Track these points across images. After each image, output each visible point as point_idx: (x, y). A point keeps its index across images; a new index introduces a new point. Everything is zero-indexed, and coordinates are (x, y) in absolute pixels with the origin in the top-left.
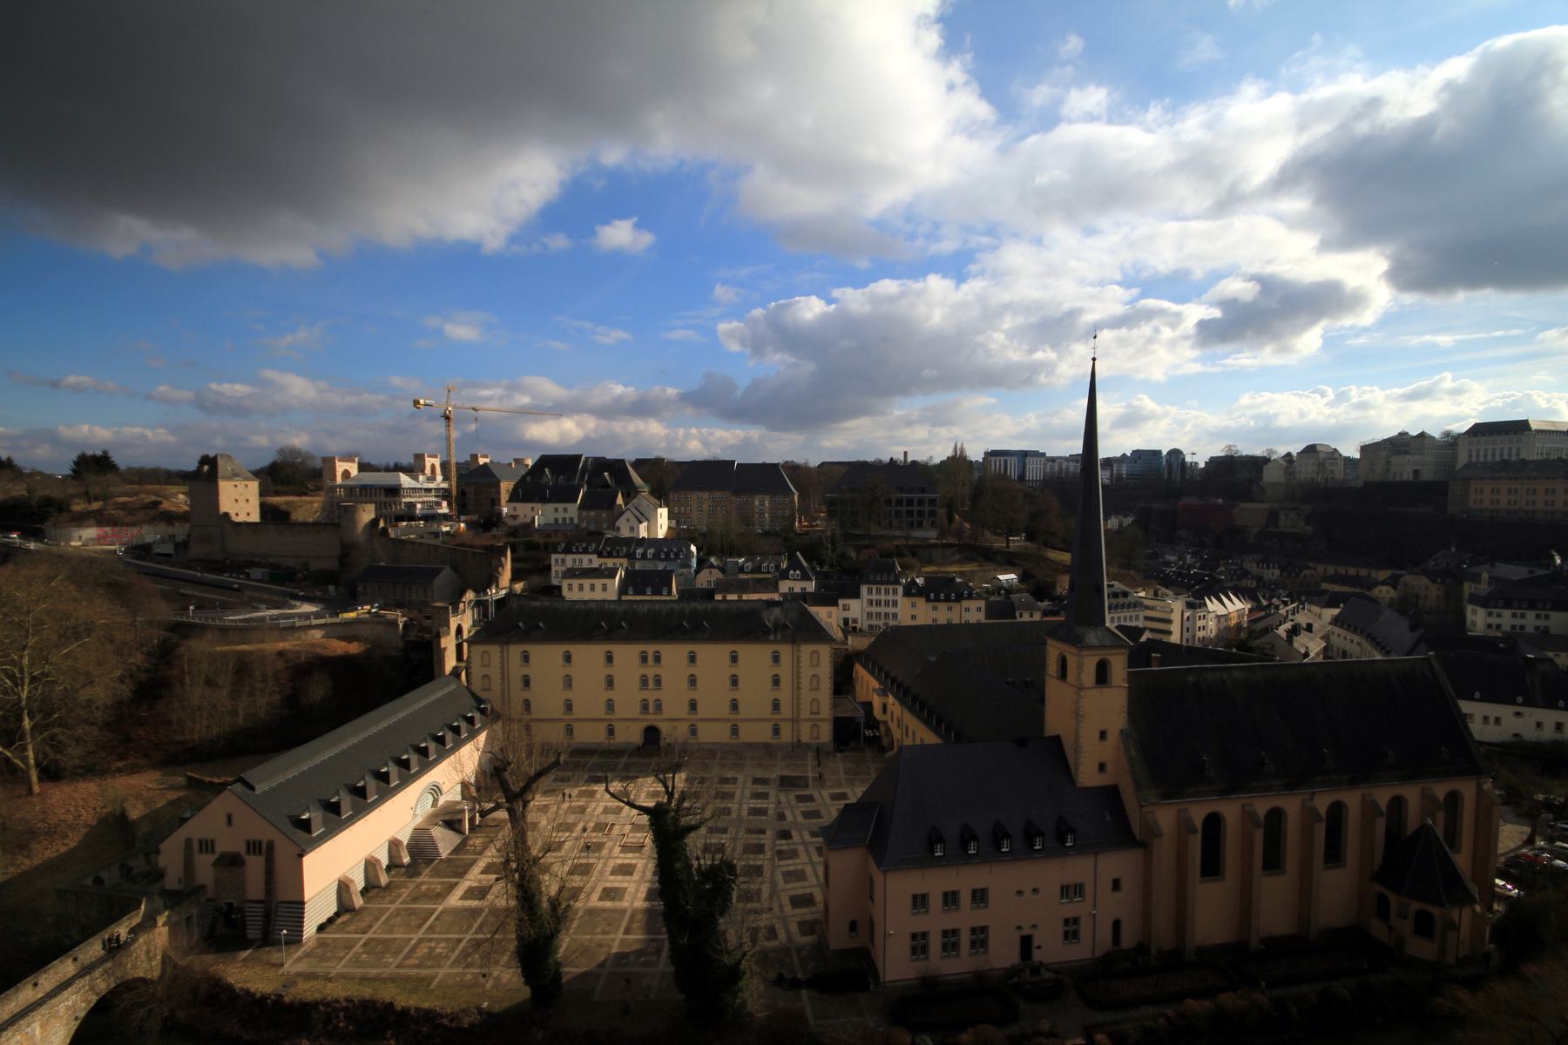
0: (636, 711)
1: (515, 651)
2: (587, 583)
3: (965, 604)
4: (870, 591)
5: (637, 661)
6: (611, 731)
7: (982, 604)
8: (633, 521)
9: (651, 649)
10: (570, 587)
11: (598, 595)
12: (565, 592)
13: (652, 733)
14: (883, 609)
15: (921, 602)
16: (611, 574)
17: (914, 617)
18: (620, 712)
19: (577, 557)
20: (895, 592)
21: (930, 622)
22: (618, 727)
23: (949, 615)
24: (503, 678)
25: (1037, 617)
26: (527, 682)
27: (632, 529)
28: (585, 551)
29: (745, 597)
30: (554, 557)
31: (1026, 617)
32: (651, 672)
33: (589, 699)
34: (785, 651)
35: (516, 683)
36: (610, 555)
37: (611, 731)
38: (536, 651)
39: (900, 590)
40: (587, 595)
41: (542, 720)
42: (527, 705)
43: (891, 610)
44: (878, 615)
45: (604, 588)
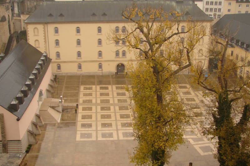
0: (113, 56)
1: (51, 28)
6: (100, 67)
9: (121, 25)
13: (121, 67)
14: (213, 7)
17: (229, 10)
18: (105, 57)
21: (237, 13)
22: (105, 65)
24: (45, 42)
26: (57, 42)
33: (89, 51)
37: (100, 67)
38: (61, 27)
41: (65, 62)
42: (58, 55)
43: (218, 7)
44: (211, 10)
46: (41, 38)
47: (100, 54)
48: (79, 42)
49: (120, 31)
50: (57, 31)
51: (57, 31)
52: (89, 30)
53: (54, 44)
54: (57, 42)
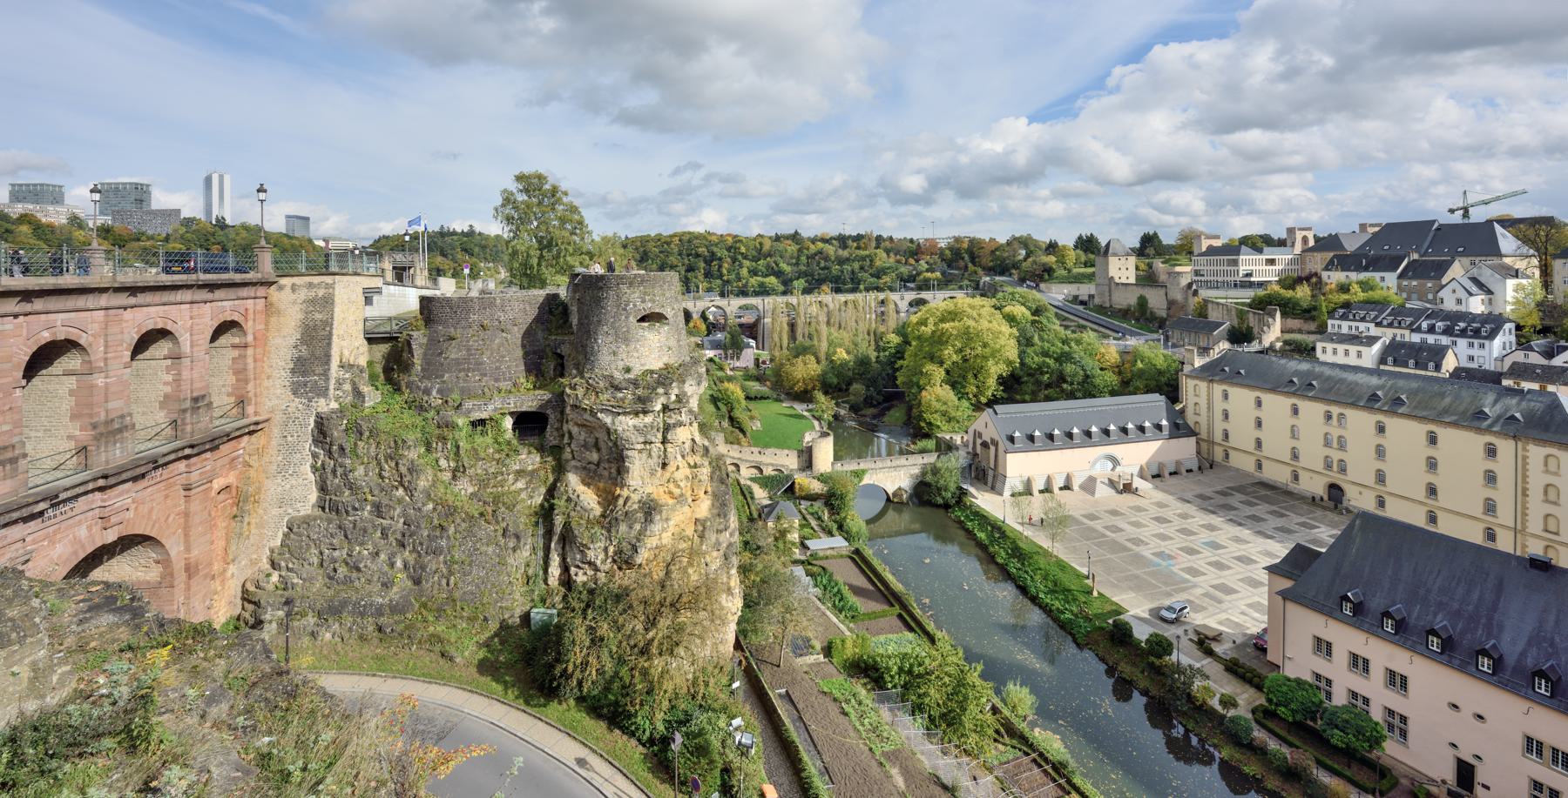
1: (1218, 389)
2: (1341, 348)
5: (1322, 419)
8: (1462, 294)
9: (1335, 410)
11: (1352, 360)
16: (1372, 340)
19: (1354, 324)
26: (1226, 416)
27: (1459, 301)
28: (1363, 319)
29: (1551, 388)
30: (1330, 322)
32: (1335, 432)
34: (1505, 447)
35: (1218, 416)
40: (1340, 359)
45: (1359, 355)
46: (1203, 402)
49: (1335, 417)
50: (1226, 396)
51: (1226, 396)
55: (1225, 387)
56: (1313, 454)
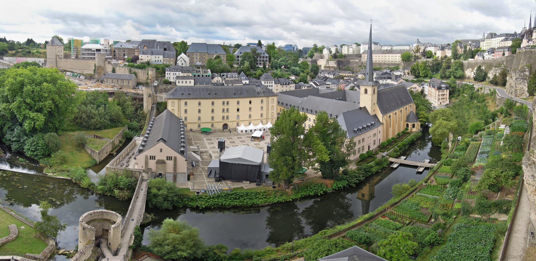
1: (183, 102)
2: (184, 81)
3: (290, 85)
4: (265, 83)
7: (294, 85)
10: (179, 82)
11: (188, 84)
12: (177, 84)
15: (279, 85)
19: (175, 73)
20: (272, 83)
23: (286, 88)
25: (306, 88)
26: (186, 111)
31: (303, 88)
32: (226, 108)
36: (185, 73)
39: (273, 82)
40: (184, 84)
45: (190, 82)
46: (176, 109)
47: (213, 118)
48: (199, 111)
50: (186, 104)
51: (186, 104)
52: (206, 104)
53: (184, 112)
54: (186, 111)
55: (184, 101)
56: (218, 116)
